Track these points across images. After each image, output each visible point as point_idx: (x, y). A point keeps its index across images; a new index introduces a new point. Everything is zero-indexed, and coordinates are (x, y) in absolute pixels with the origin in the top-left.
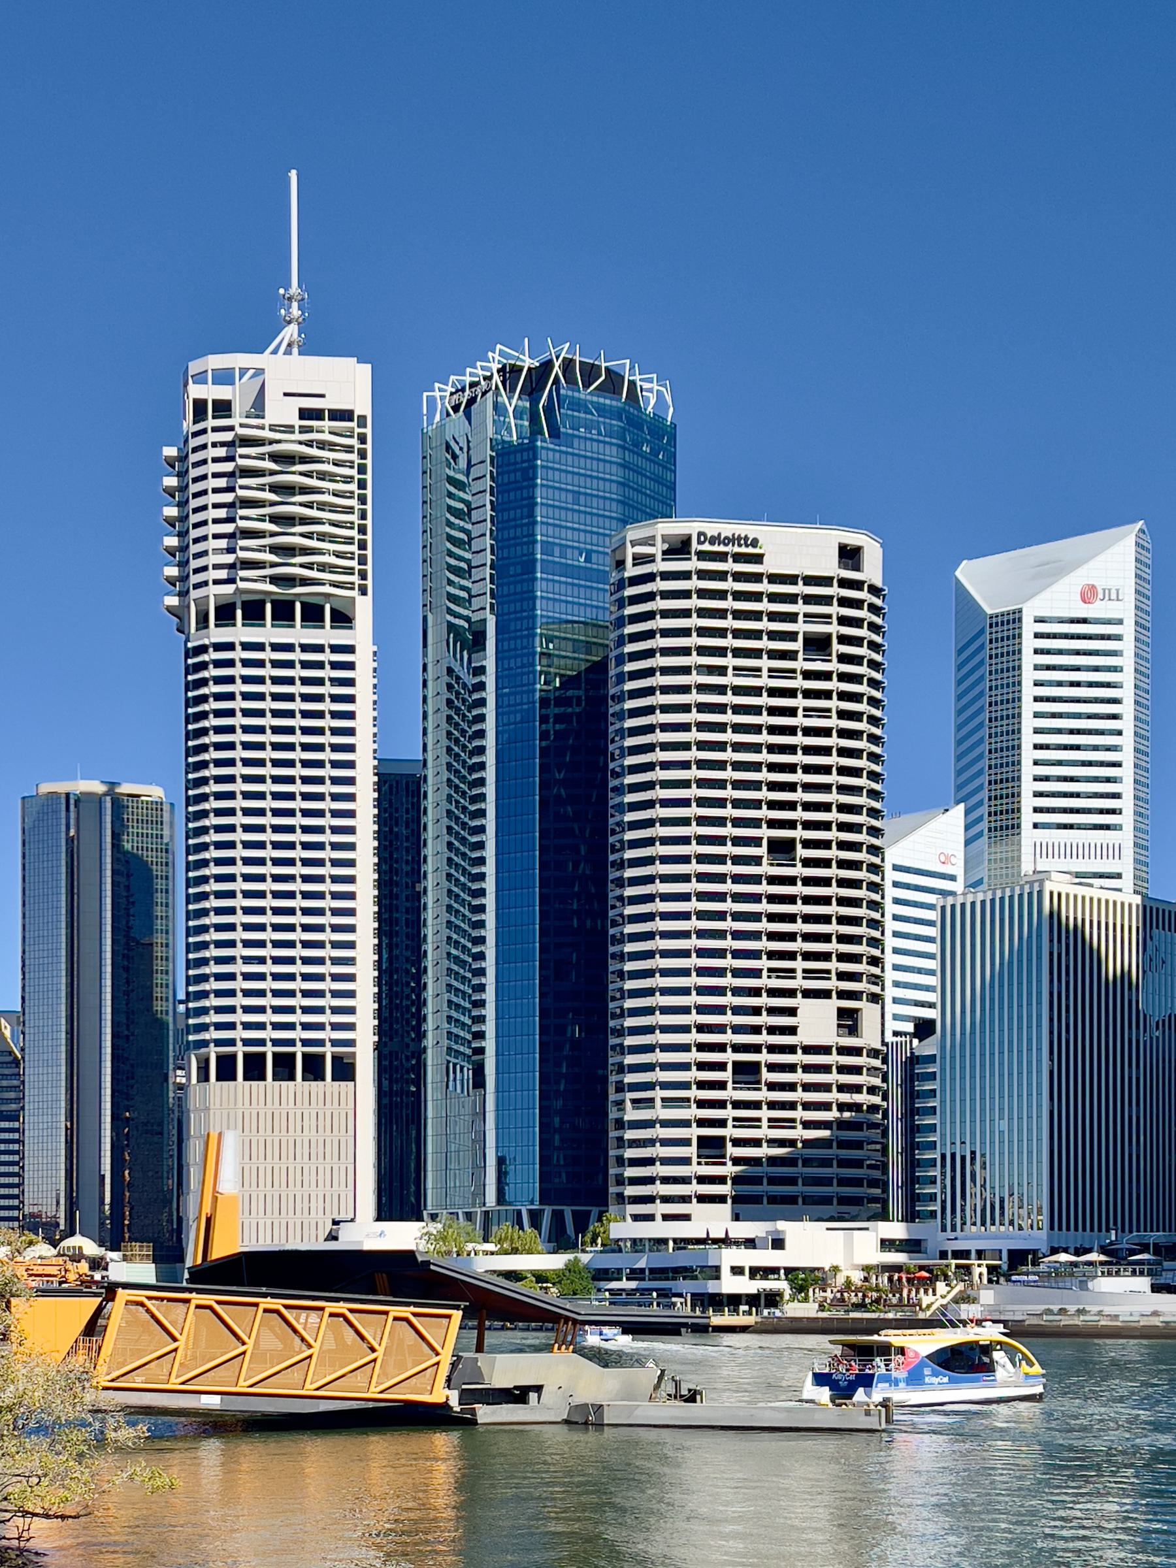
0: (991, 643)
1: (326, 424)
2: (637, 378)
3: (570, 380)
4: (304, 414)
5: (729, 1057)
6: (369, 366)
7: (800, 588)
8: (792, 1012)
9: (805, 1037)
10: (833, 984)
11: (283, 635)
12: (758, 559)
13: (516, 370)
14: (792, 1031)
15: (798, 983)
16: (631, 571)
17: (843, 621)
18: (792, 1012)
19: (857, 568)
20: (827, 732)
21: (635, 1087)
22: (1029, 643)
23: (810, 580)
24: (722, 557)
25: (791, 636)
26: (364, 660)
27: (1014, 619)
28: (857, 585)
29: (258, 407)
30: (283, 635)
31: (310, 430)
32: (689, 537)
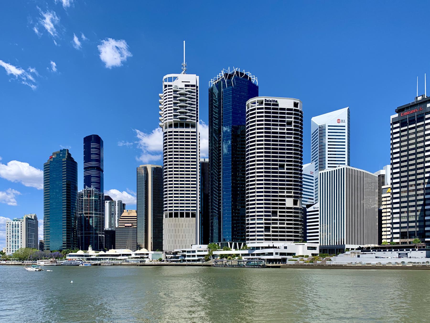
1: (190, 87)
2: (251, 76)
4: (186, 86)
5: (271, 210)
8: (284, 200)
9: (287, 206)
13: (227, 74)
14: (284, 204)
15: (285, 194)
16: (250, 108)
18: (284, 200)
19: (297, 107)
21: (251, 216)
31: (187, 89)
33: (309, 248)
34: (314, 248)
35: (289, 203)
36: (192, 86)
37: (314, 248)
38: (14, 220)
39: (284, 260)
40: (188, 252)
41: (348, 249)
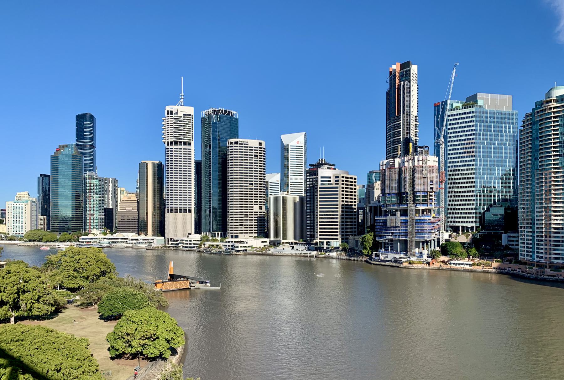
0: (284, 149)
4: (184, 115)
6: (193, 108)
11: (180, 147)
13: (215, 111)
22: (290, 149)
26: (193, 151)
27: (288, 146)
29: (177, 113)
30: (180, 147)
33: (262, 242)
34: (265, 242)
36: (188, 115)
37: (265, 242)
38: (15, 202)
41: (283, 243)
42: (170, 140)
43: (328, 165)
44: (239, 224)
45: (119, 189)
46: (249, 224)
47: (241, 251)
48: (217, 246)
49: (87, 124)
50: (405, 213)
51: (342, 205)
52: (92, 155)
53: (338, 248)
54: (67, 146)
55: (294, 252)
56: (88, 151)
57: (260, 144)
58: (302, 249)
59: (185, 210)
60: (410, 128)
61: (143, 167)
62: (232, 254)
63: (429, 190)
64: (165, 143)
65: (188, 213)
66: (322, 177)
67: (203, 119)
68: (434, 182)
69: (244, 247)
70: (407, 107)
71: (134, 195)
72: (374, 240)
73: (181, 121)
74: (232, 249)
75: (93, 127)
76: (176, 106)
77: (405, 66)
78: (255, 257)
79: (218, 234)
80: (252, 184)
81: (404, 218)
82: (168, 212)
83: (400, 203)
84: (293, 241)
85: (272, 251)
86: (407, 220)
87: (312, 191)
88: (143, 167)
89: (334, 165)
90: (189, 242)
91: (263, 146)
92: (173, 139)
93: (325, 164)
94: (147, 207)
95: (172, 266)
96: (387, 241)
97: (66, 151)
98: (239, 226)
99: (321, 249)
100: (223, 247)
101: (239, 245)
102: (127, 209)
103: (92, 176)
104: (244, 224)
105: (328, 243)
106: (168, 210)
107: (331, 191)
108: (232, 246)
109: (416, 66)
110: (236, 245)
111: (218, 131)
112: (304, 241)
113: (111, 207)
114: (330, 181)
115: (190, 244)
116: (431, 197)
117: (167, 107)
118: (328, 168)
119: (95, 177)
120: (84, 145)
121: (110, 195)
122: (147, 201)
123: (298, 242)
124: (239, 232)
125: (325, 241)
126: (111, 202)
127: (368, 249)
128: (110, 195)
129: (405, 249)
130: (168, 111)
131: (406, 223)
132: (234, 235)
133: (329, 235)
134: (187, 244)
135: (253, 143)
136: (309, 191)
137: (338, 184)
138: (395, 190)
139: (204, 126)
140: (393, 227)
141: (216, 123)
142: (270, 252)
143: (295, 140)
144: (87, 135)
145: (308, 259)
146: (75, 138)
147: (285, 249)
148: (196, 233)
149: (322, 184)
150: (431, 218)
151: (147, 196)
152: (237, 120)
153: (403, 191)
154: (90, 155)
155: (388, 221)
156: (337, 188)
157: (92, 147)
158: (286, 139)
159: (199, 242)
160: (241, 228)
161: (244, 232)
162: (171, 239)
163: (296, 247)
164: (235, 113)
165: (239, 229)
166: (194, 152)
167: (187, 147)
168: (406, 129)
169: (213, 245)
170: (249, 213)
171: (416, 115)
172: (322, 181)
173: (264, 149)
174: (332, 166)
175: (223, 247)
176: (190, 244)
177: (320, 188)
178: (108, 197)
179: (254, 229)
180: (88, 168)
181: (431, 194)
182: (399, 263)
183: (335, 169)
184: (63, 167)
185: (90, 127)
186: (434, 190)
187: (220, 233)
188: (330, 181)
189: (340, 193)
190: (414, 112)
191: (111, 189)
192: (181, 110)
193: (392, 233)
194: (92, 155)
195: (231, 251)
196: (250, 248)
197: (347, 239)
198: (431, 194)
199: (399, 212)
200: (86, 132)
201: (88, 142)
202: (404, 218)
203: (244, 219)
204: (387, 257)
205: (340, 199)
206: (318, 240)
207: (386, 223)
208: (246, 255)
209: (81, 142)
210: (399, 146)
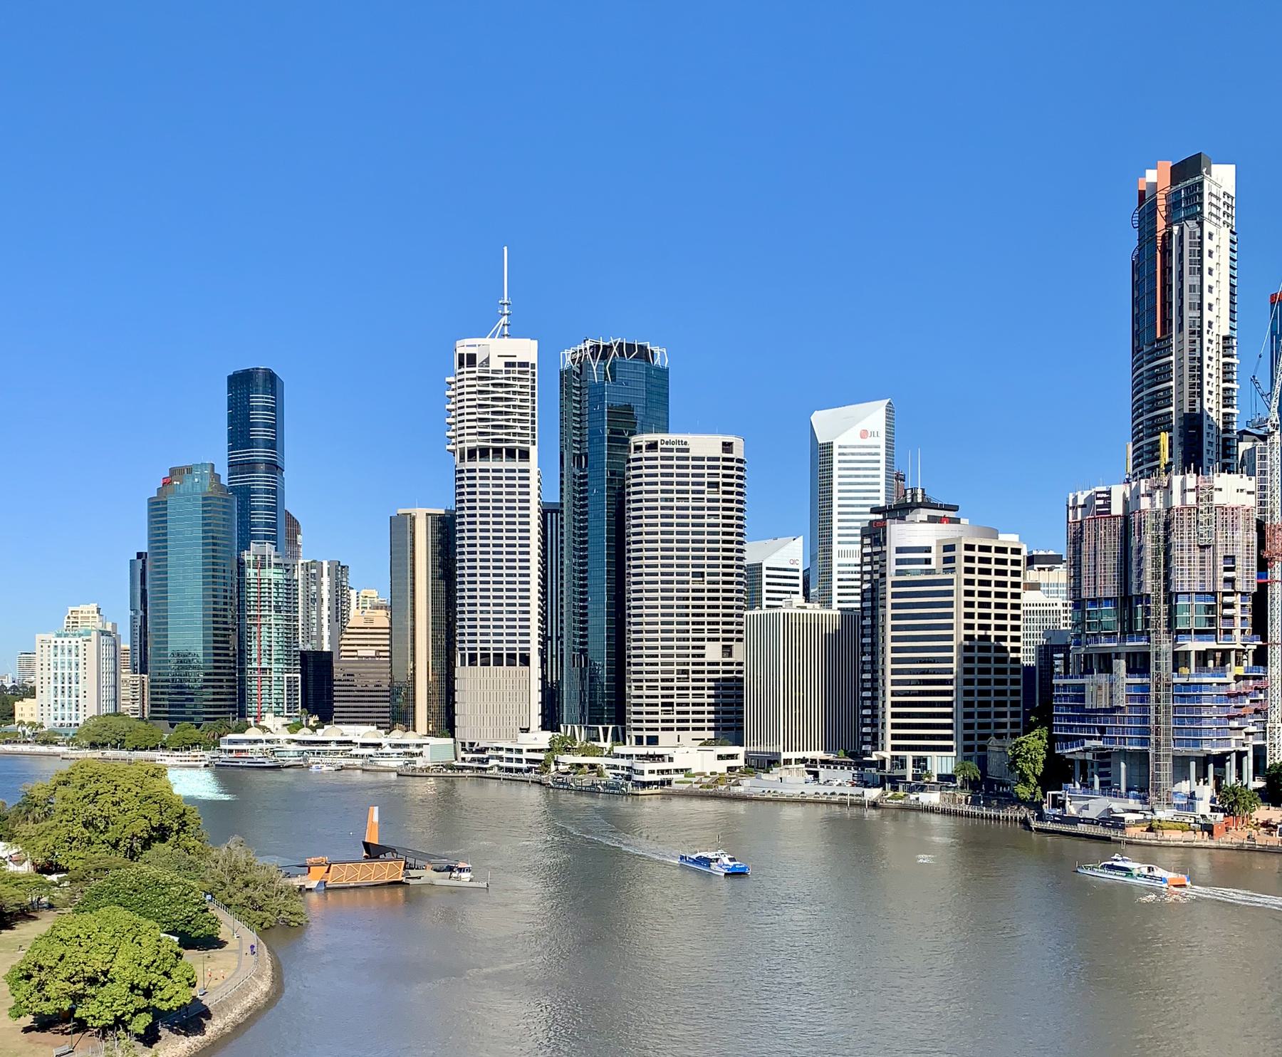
1: (517, 369)
3: (621, 354)
4: (507, 364)
7: (706, 463)
10: (720, 635)
11: (497, 465)
12: (687, 450)
15: (706, 635)
17: (724, 476)
20: (717, 525)
23: (709, 459)
24: (672, 450)
25: (702, 484)
26: (534, 476)
28: (731, 460)
29: (487, 360)
30: (497, 465)
32: (656, 443)
33: (720, 757)
35: (713, 652)
39: (669, 782)
40: (510, 750)
41: (788, 761)
42: (467, 445)
43: (934, 507)
44: (660, 701)
45: (353, 593)
46: (691, 700)
47: (655, 783)
48: (592, 766)
49: (259, 399)
50: (1139, 663)
51: (967, 637)
52: (274, 492)
53: (951, 778)
54: (190, 470)
55: (811, 789)
56: (259, 480)
57: (727, 447)
58: (840, 781)
59: (511, 657)
60: (1201, 377)
61: (401, 527)
62: (625, 794)
63: (1221, 587)
64: (453, 452)
65: (518, 668)
66: (899, 550)
67: (565, 376)
68: (1238, 562)
69: (662, 772)
70: (1191, 307)
71: (383, 612)
72: (1050, 751)
73: (501, 385)
74: (628, 778)
75: (275, 409)
76: (487, 340)
77: (1188, 171)
78: (696, 804)
79: (605, 730)
80: (702, 574)
81: (1138, 680)
82: (463, 664)
83: (1129, 630)
84: (820, 755)
85: (747, 785)
86: (1145, 687)
87: (872, 596)
88: (401, 527)
89: (955, 508)
90: (514, 756)
91: (738, 453)
92: (477, 442)
93: (919, 506)
94: (414, 648)
95: (376, 818)
96: (1089, 756)
97: (188, 483)
98: (659, 708)
99: (895, 781)
100: (607, 772)
101: (648, 766)
102: (360, 653)
103: (263, 557)
104: (675, 700)
105: (920, 763)
106: (463, 656)
107: (931, 595)
108: (629, 768)
109: (1231, 169)
110: (639, 766)
111: (608, 411)
112: (852, 755)
113: (326, 648)
114: (928, 561)
115: (519, 761)
116: (1227, 612)
117: (459, 343)
118: (932, 520)
119: (273, 560)
120: (249, 463)
121: (325, 613)
122: (414, 629)
123: (831, 757)
124: (660, 725)
125: (909, 755)
126: (326, 633)
127: (1033, 780)
128: (325, 613)
129: (1142, 787)
130: (461, 356)
131: (1144, 698)
132: (645, 734)
133: (916, 737)
134: (510, 760)
135: (706, 445)
136: (868, 595)
137: (952, 570)
138: (1109, 589)
139: (569, 398)
140: (1105, 710)
141: (601, 385)
142: (740, 790)
143: (856, 431)
144: (259, 433)
145: (849, 812)
146: (224, 443)
147: (792, 781)
148: (544, 727)
149: (899, 573)
150: (1229, 678)
151: (414, 616)
152: (664, 373)
153: (1134, 592)
154: (267, 492)
155: (1089, 690)
156: (950, 582)
157: (274, 467)
158: (825, 423)
159: (541, 756)
160: (667, 712)
161: (675, 725)
162: (472, 744)
163: (823, 773)
164: (657, 350)
165: (660, 717)
166: (539, 478)
167: (517, 464)
168: (1187, 381)
169: (580, 766)
170: (691, 668)
171: (1227, 332)
172: (899, 562)
173: (739, 461)
174: (945, 512)
175: (607, 772)
176: (519, 761)
177: (895, 584)
178: (320, 618)
179: (706, 716)
180: (262, 531)
181: (1227, 599)
182: (1115, 827)
183: (957, 521)
184: (179, 532)
185: (266, 408)
186: (1240, 586)
187: (611, 727)
188: (928, 561)
189: (959, 599)
190: (1218, 320)
191: (326, 596)
192: (497, 349)
193: (1102, 730)
194: (274, 492)
195: (627, 785)
196: (681, 777)
197: (983, 748)
198: (1227, 599)
199: (1123, 662)
200: (253, 425)
201: (260, 454)
202: (1138, 680)
203: (675, 684)
204: (1086, 807)
205: (959, 621)
206: (887, 754)
207: (1082, 698)
208: (667, 796)
209: (242, 455)
210: (1164, 438)
